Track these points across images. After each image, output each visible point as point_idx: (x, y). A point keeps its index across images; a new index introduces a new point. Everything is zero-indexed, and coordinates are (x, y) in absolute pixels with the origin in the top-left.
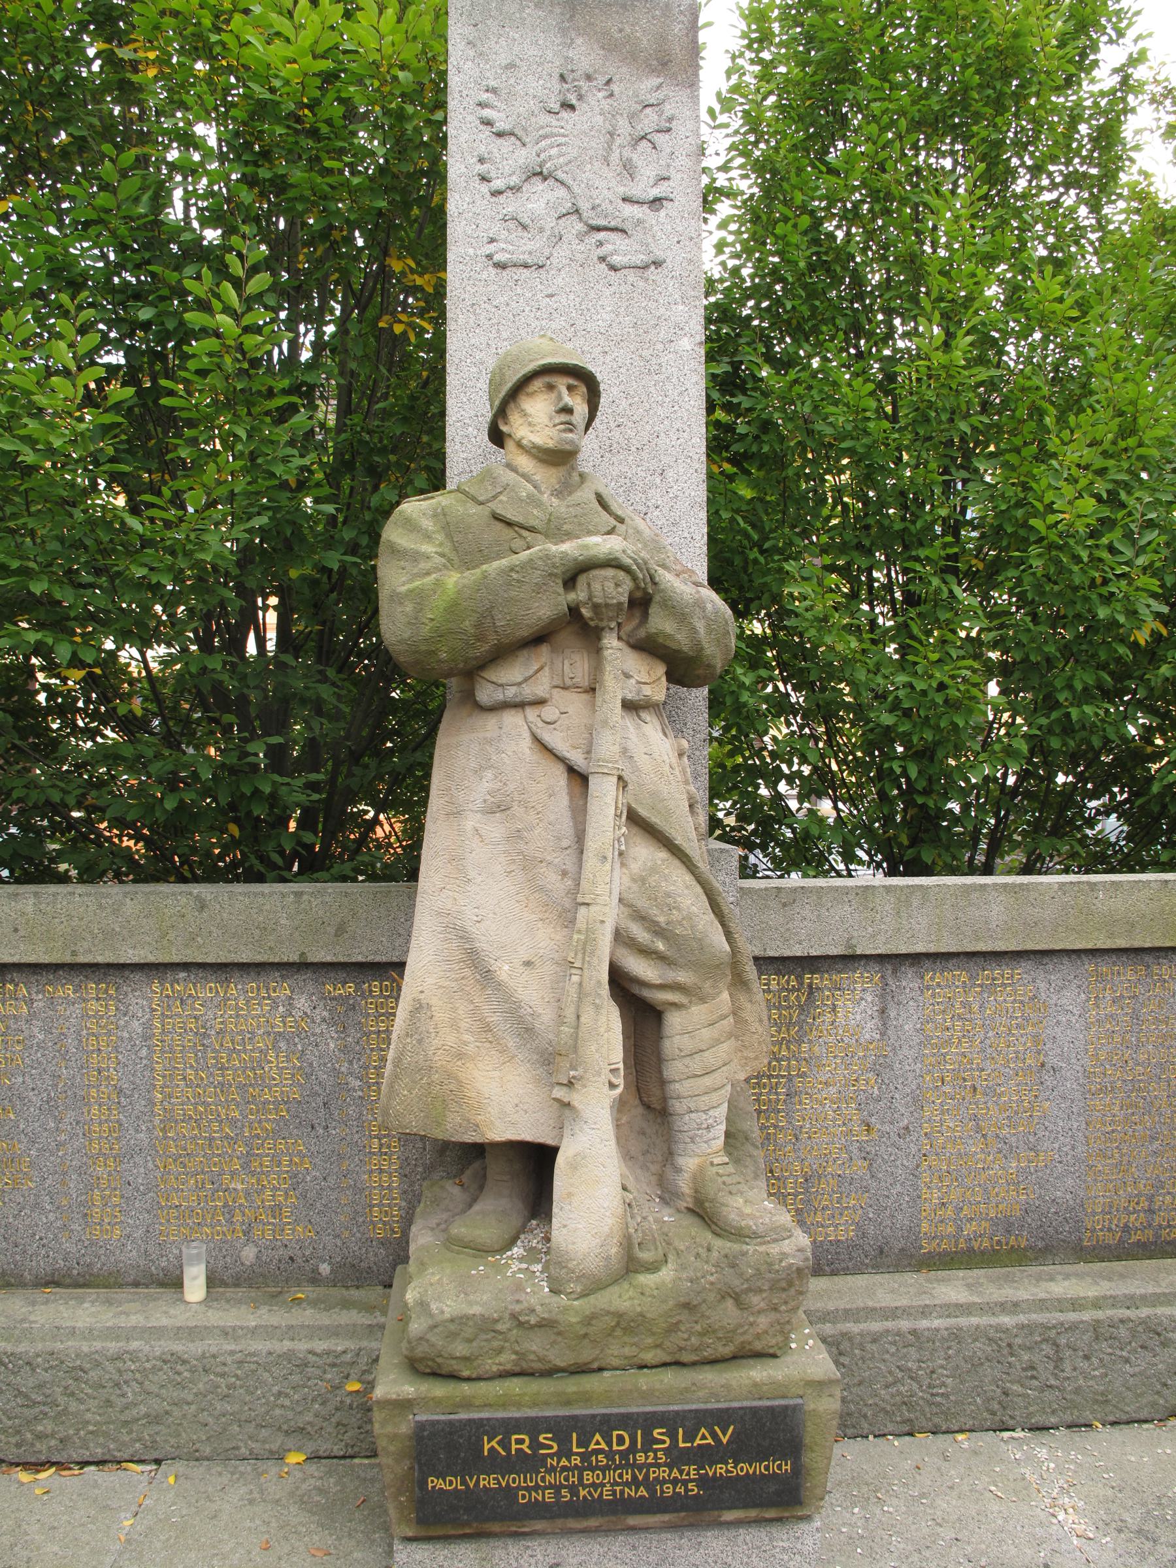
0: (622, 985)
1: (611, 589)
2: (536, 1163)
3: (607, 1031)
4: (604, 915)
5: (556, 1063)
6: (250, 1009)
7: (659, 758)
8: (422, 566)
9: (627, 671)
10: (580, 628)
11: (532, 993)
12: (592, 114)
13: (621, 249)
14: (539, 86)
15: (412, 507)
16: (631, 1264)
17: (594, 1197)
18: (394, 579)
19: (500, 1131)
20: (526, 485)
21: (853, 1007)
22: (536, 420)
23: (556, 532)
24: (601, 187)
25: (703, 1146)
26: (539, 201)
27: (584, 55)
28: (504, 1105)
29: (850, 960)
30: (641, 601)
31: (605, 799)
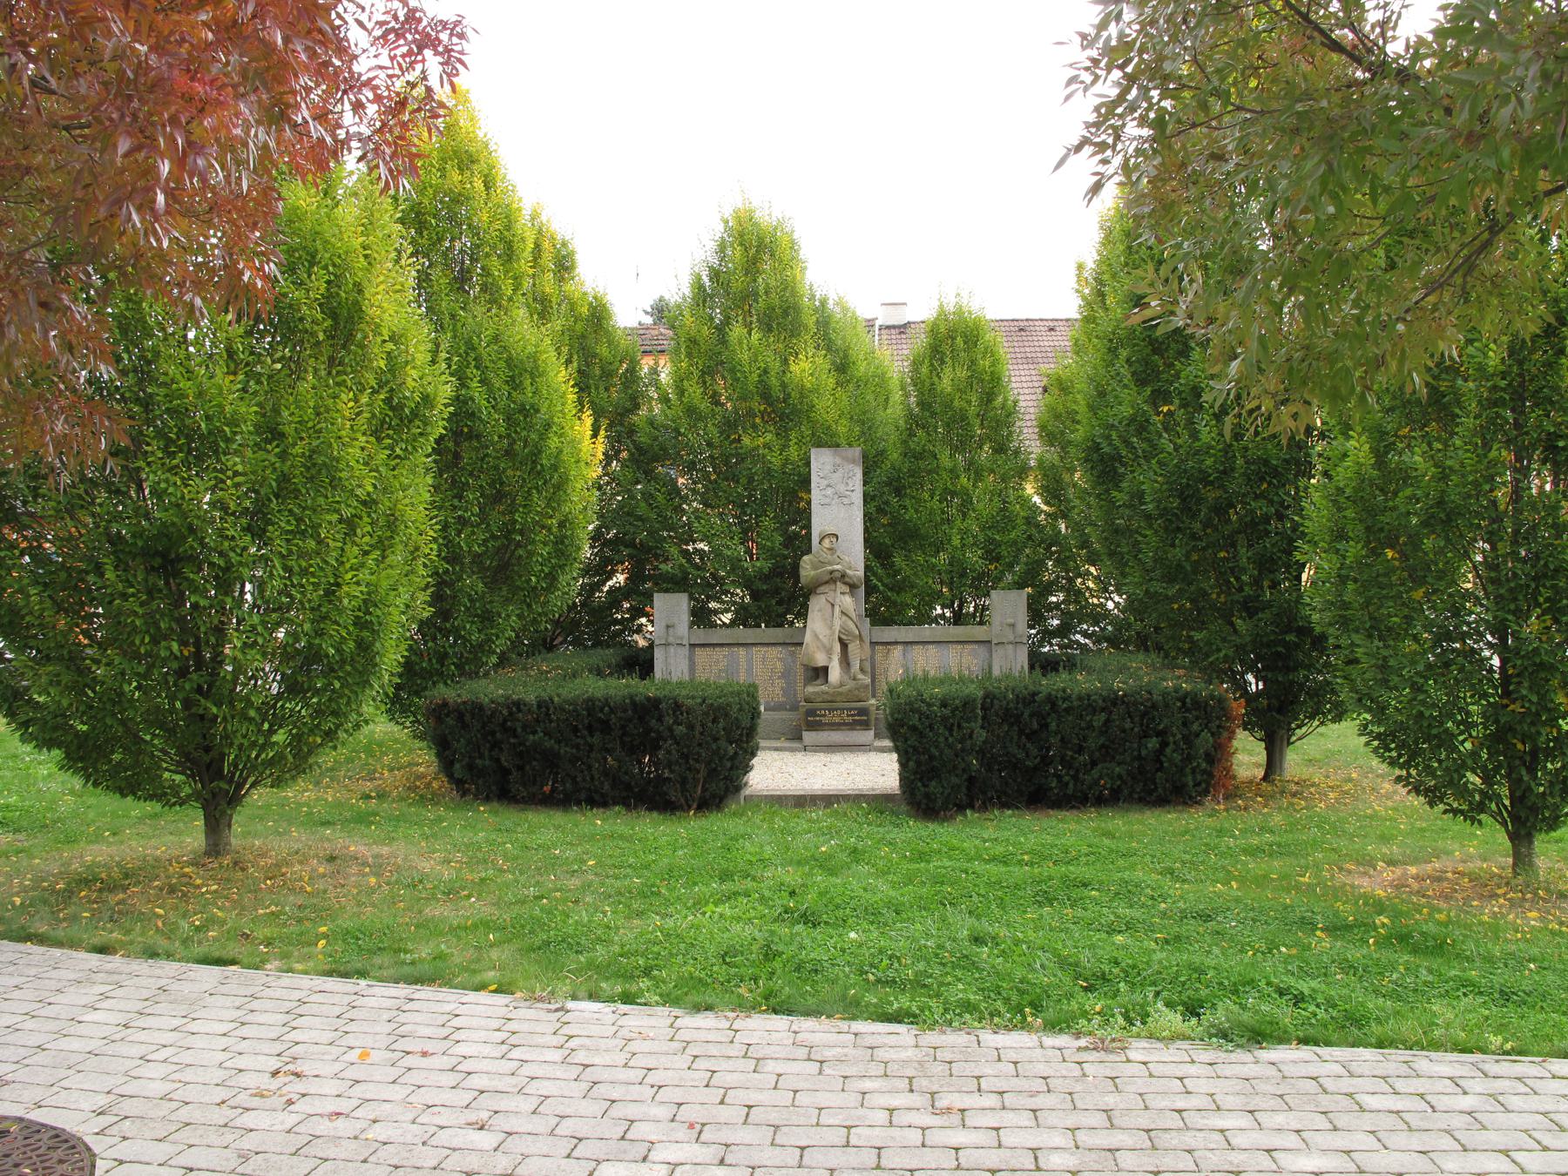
0: (840, 640)
1: (837, 575)
2: (825, 669)
3: (837, 647)
4: (837, 628)
5: (829, 652)
6: (774, 652)
7: (849, 603)
8: (808, 569)
9: (841, 587)
10: (832, 581)
11: (825, 641)
12: (839, 474)
13: (846, 501)
14: (829, 467)
15: (805, 558)
16: (841, 685)
17: (835, 674)
18: (803, 573)
19: (820, 664)
20: (827, 557)
21: (897, 652)
22: (826, 543)
23: (831, 564)
24: (842, 488)
25: (856, 666)
26: (829, 492)
27: (838, 460)
28: (820, 660)
29: (896, 643)
30: (843, 576)
31: (837, 609)
